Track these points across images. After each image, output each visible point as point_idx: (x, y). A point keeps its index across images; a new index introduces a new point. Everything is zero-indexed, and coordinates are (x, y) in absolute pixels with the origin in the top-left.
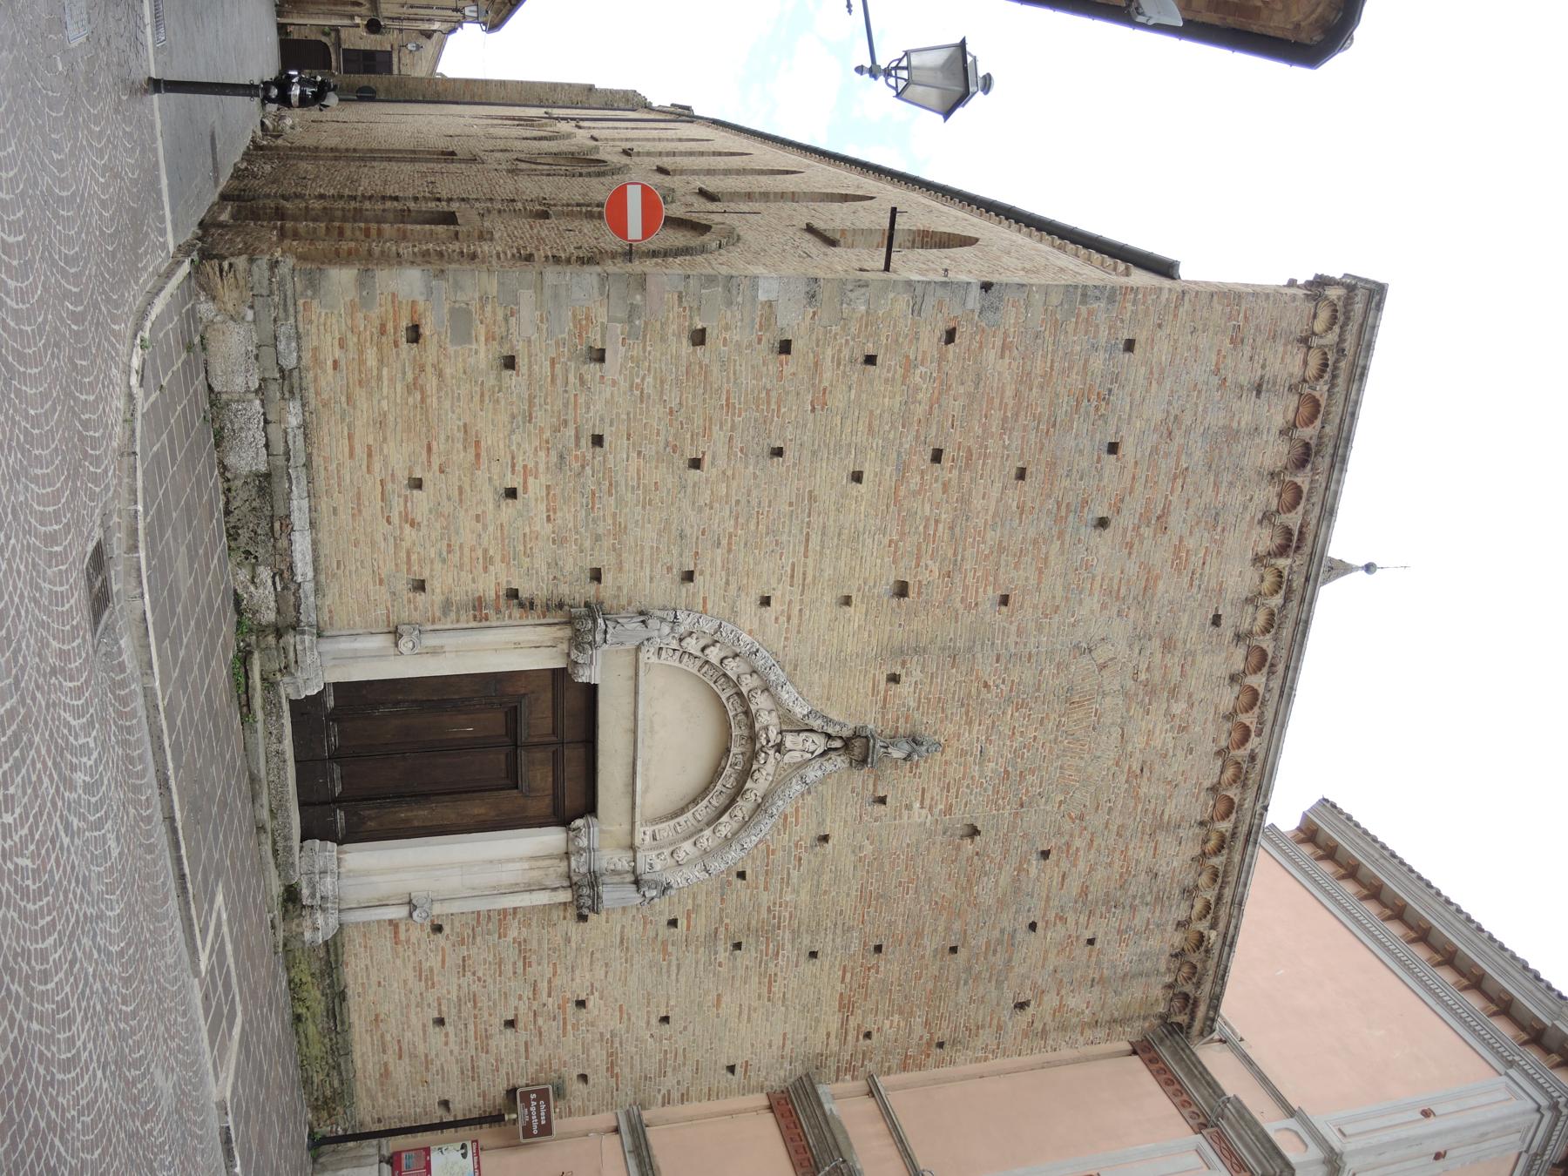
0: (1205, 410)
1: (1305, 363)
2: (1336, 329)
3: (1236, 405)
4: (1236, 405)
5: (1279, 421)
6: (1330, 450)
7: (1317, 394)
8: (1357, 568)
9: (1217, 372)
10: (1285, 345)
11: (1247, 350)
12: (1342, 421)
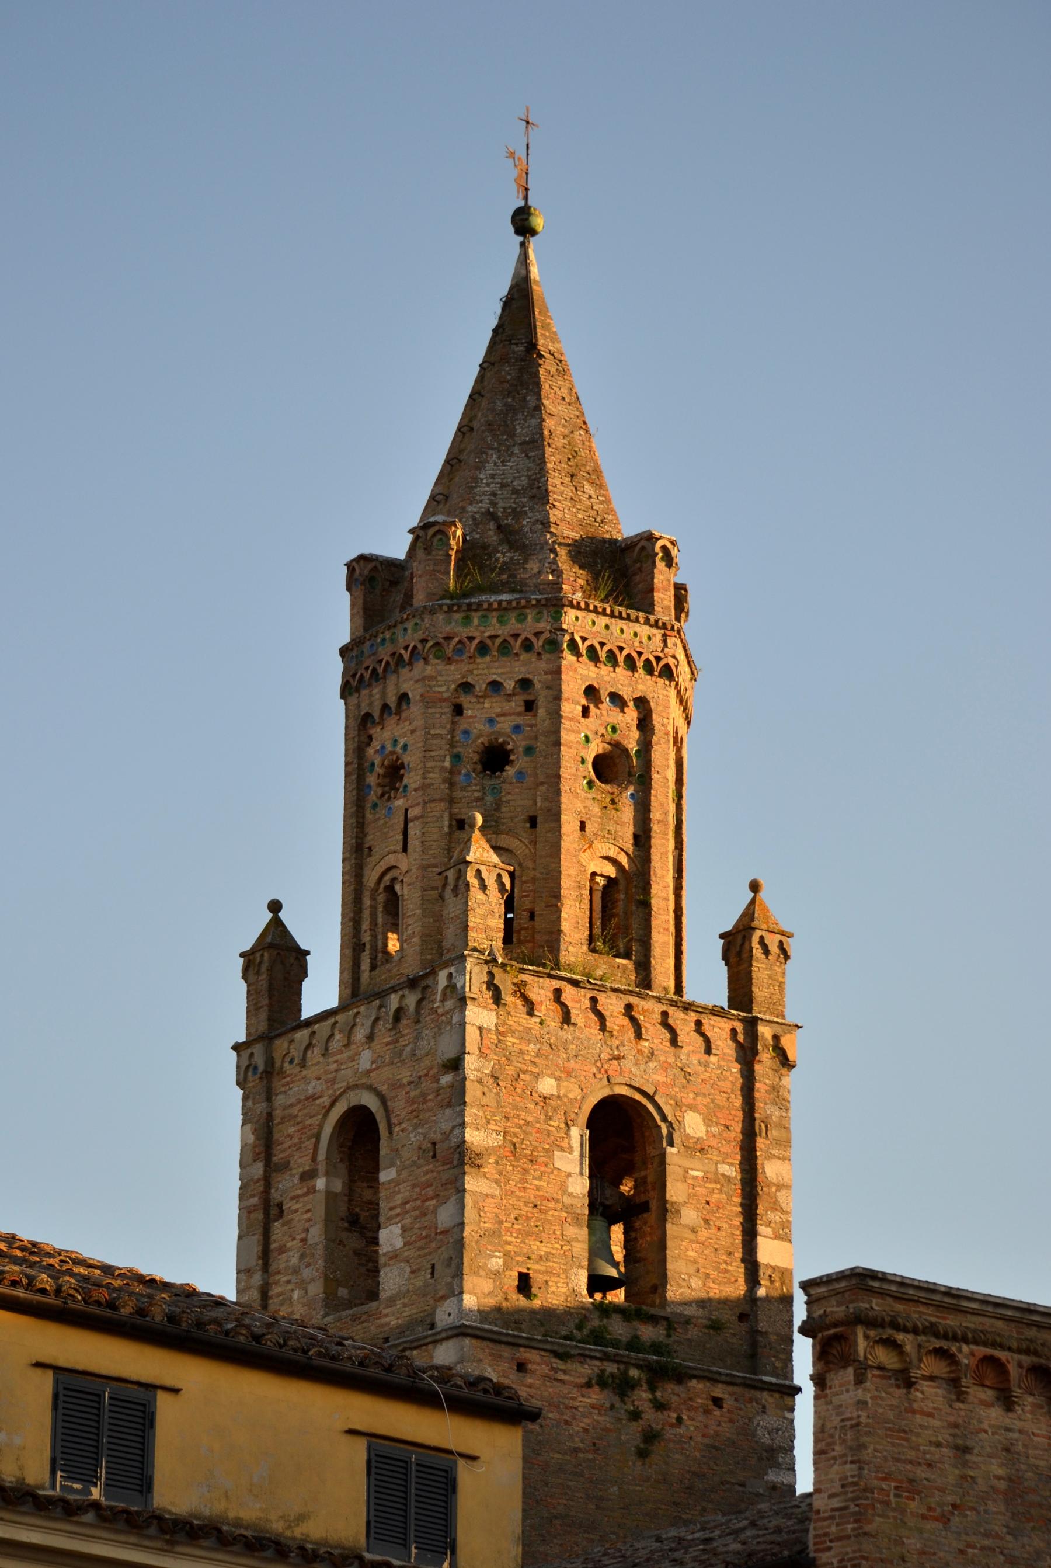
0: (987, 1535)
1: (932, 1378)
2: (900, 1337)
3: (982, 1486)
4: (982, 1486)
5: (996, 1414)
6: (1032, 1333)
7: (973, 1362)
8: (524, 260)
9: (944, 1519)
10: (914, 1412)
11: (921, 1473)
12: (1002, 1318)
